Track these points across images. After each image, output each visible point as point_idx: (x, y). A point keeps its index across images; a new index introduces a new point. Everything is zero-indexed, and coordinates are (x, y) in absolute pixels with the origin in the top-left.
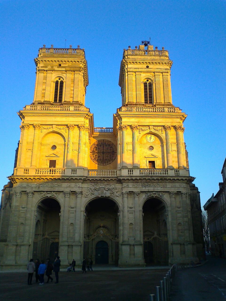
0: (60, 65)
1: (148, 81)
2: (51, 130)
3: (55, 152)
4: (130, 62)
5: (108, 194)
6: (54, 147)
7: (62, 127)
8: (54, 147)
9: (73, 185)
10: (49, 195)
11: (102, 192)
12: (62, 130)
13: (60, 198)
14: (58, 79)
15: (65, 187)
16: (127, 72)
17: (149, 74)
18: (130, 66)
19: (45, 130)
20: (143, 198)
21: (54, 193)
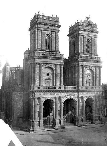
0: (48, 27)
1: (88, 41)
2: (47, 66)
3: (48, 77)
4: (82, 30)
5: (73, 97)
6: (48, 75)
7: (52, 65)
8: (48, 75)
9: (59, 93)
10: (49, 99)
11: (71, 96)
12: (53, 66)
13: (53, 99)
14: (47, 35)
15: (56, 95)
16: (80, 35)
17: (88, 37)
18: (81, 32)
19: (45, 66)
20: (85, 99)
21: (51, 98)
